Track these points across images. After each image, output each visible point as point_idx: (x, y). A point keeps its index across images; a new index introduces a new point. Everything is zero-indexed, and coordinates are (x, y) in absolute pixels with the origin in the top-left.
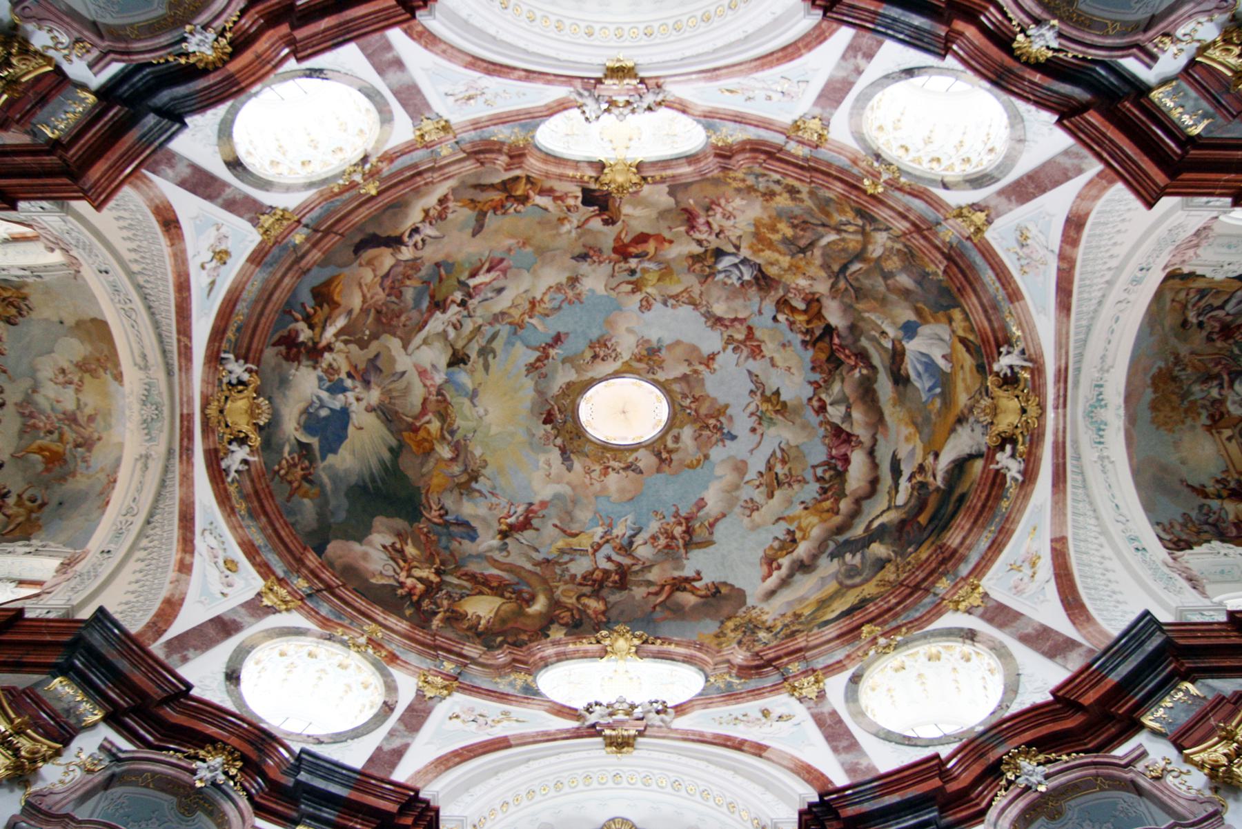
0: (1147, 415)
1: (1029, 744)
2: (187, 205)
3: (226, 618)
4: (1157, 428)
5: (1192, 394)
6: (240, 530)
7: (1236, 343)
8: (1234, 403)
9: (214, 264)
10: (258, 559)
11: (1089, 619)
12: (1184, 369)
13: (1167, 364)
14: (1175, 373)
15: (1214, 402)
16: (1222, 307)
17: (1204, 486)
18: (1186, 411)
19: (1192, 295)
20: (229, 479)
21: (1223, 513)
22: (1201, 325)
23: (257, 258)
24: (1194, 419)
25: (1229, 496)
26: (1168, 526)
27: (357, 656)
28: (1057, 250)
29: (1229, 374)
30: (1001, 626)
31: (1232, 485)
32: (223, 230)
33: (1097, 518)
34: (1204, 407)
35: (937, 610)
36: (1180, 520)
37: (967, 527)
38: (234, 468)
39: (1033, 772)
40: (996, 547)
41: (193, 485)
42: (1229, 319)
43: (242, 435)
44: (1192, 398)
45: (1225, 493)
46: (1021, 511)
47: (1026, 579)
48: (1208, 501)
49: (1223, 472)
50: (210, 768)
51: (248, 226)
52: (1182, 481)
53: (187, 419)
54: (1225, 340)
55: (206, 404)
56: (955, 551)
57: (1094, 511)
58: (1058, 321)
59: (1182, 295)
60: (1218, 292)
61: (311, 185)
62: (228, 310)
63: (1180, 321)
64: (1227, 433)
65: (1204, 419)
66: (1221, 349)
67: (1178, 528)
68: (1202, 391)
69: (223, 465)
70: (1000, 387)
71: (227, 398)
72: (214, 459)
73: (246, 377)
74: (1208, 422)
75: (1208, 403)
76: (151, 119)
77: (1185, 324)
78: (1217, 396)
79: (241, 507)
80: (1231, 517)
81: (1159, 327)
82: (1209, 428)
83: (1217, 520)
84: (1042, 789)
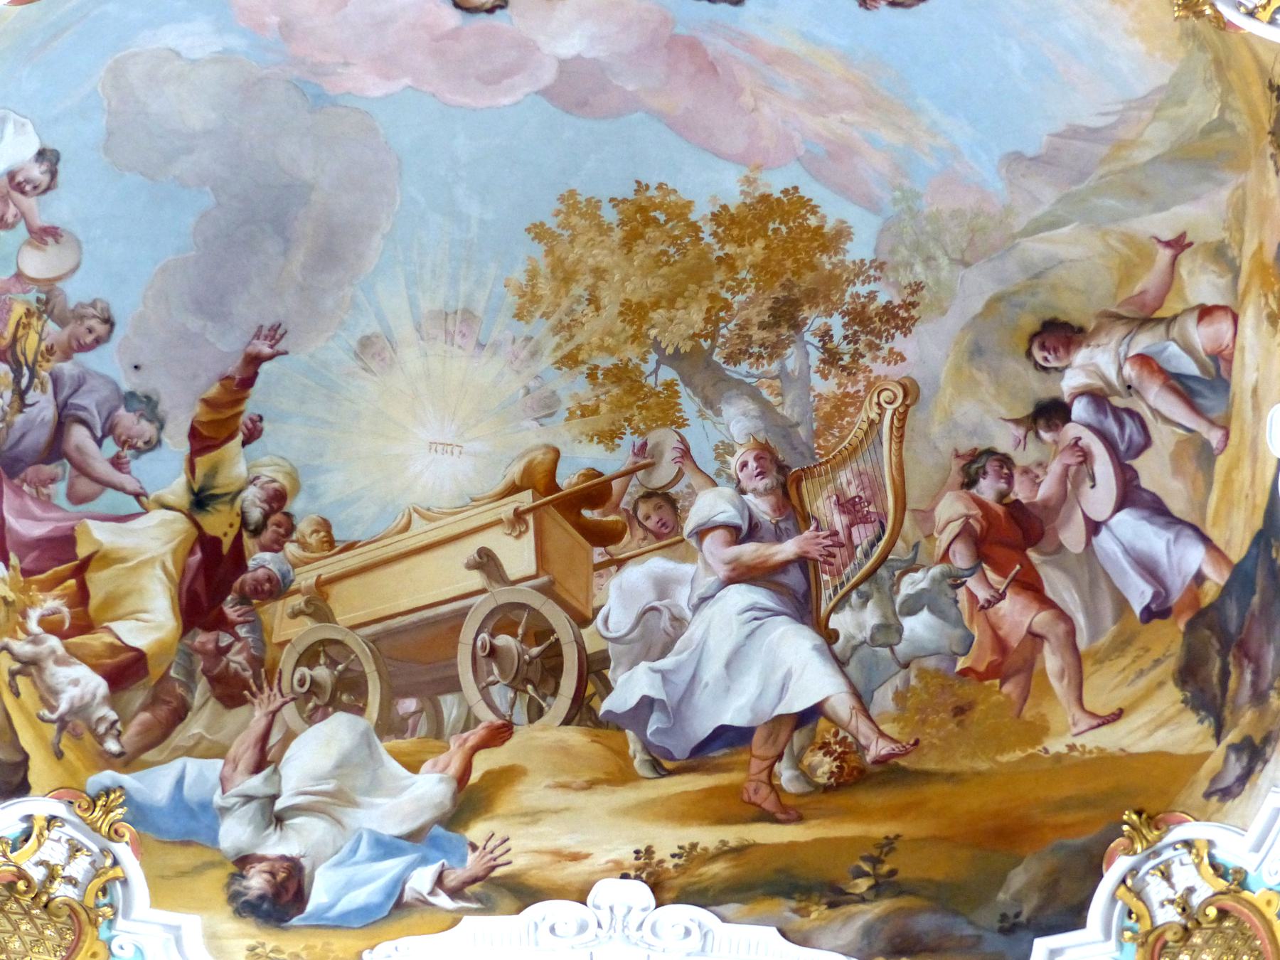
0: (607, 180)
4: (539, 232)
5: (710, 404)
7: (956, 581)
8: (663, 587)
12: (831, 358)
13: (860, 271)
14: (814, 320)
15: (667, 502)
16: (1130, 494)
17: (252, 435)
18: (623, 375)
19: (1201, 335)
21: (110, 501)
22: (1052, 413)
24: (587, 411)
25: (207, 543)
26: (44, 211)
29: (802, 561)
31: (261, 561)
34: (646, 458)
36: (75, 292)
42: (1072, 536)
44: (688, 404)
45: (219, 523)
48: (176, 444)
49: (325, 525)
52: (275, 334)
54: (966, 532)
59: (1202, 285)
60: (1206, 455)
63: (1074, 310)
64: (518, 555)
65: (582, 458)
66: (926, 516)
67: (36, 264)
68: (723, 450)
74: (567, 478)
75: (661, 477)
77: (1060, 335)
78: (691, 522)
80: (99, 535)
81: (1047, 196)
82: (539, 478)
83: (82, 470)
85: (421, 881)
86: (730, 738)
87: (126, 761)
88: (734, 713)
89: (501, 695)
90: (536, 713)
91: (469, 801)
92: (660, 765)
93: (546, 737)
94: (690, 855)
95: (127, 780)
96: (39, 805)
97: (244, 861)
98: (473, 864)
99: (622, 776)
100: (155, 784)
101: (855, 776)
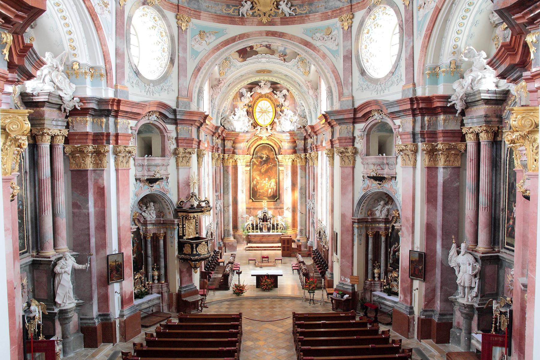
2: (191, 67)
3: (345, 54)
6: (316, 16)
9: (206, 39)
10: (330, 14)
20: (294, 14)
23: (197, 14)
27: (381, 5)
32: (193, 43)
38: (288, 10)
41: (294, 36)
43: (275, 3)
50: (377, 117)
51: (188, 30)
53: (268, 33)
55: (261, 23)
61: (164, 16)
62: (222, 18)
69: (288, 16)
71: (258, 10)
72: (286, 20)
73: (249, 3)
76: (178, 117)
79: (306, 8)
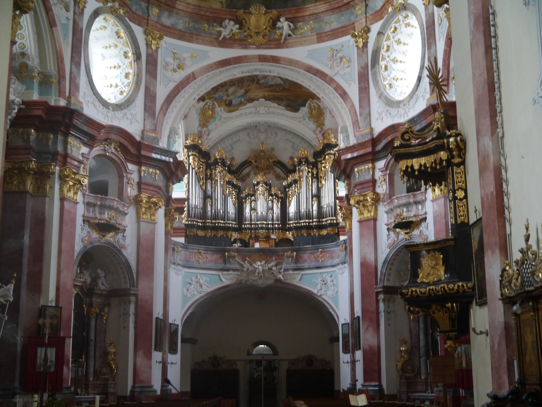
1: (120, 142)
11: (165, 114)
28: (335, 78)
30: (147, 71)
33: (206, 81)
35: (142, 20)
37: (189, 10)
39: (111, 150)
40: (181, 35)
46: (204, 43)
47: (171, 67)
56: (174, 8)
57: (209, 79)
58: (304, 64)
70: (271, 18)
84: (107, 154)
85: (243, 100)
86: (272, 86)
87: (214, 94)
88: (273, 83)
89: (249, 83)
90: (253, 84)
91: (247, 92)
92: (265, 87)
93: (254, 86)
94: (268, 95)
95: (215, 96)
96: (206, 101)
97: (226, 101)
98: (247, 97)
99: (261, 88)
100: (217, 95)
101: (284, 89)
